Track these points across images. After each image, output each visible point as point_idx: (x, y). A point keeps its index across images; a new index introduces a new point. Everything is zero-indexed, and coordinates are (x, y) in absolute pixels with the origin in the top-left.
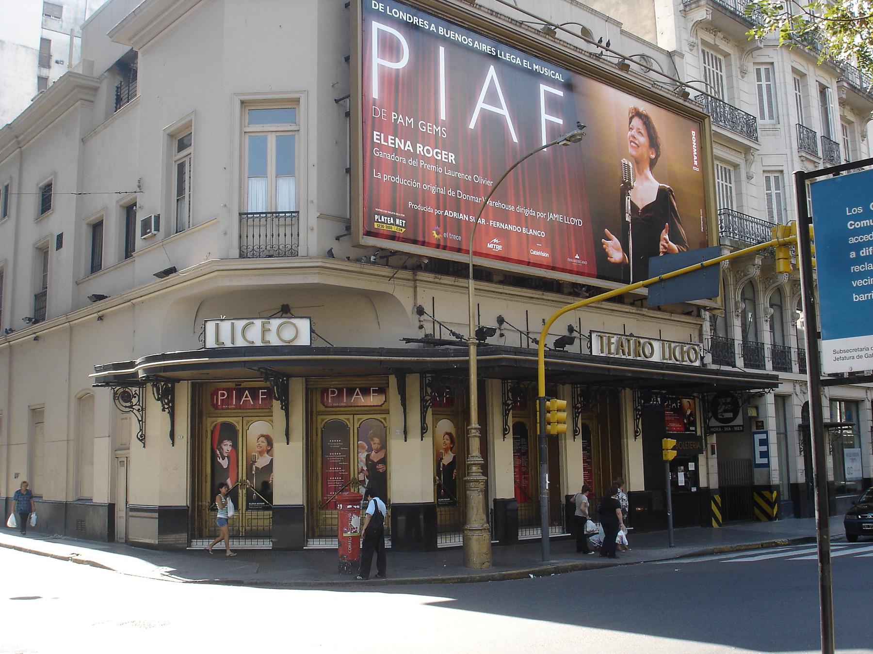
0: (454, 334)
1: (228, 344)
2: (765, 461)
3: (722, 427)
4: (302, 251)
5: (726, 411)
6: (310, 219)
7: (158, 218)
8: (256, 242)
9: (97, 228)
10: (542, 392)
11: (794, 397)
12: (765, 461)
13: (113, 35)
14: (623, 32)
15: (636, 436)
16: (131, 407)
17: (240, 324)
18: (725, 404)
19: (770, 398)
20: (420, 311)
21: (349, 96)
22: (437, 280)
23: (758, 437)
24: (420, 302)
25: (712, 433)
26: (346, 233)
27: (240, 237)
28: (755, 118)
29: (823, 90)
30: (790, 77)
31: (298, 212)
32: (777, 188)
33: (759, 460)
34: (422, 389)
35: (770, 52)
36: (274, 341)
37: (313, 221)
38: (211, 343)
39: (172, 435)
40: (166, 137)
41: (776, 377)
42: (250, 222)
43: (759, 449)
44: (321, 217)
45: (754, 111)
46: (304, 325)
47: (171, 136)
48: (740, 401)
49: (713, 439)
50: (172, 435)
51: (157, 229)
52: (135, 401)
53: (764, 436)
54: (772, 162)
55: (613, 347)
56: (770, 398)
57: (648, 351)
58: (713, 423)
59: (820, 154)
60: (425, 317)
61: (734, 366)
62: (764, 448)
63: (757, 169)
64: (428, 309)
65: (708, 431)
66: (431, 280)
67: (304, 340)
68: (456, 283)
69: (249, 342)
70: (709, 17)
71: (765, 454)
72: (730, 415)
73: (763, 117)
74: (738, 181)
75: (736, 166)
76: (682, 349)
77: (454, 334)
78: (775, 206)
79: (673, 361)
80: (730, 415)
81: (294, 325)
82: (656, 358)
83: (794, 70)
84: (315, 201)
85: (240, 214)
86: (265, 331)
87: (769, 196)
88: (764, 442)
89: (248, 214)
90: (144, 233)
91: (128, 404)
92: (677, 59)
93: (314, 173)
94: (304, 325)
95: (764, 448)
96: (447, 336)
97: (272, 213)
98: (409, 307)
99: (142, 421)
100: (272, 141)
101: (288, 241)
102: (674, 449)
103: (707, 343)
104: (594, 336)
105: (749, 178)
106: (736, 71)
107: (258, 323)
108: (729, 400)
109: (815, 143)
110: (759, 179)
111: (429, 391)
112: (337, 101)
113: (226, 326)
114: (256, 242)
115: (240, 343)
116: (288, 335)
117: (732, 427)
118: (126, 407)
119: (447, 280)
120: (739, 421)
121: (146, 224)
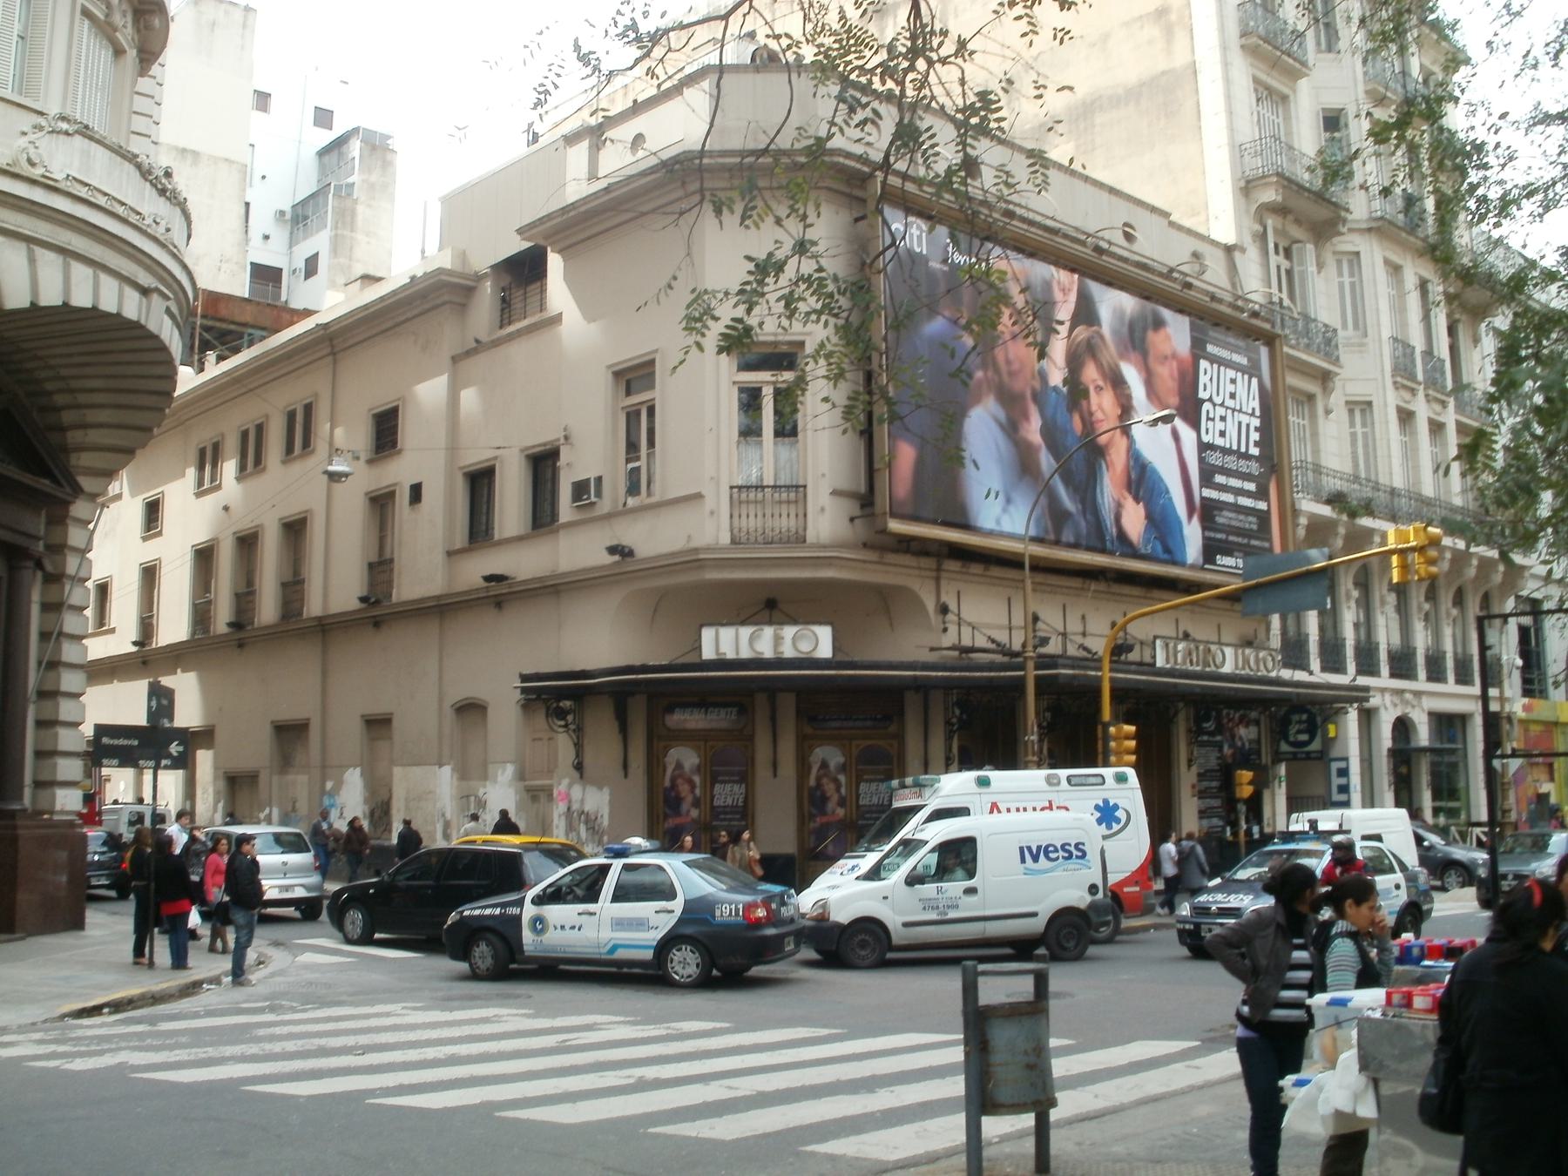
0: (993, 641)
1: (730, 655)
2: (1343, 797)
3: (1295, 754)
4: (811, 537)
5: (1299, 732)
7: (599, 480)
9: (480, 482)
10: (1107, 714)
11: (1382, 711)
12: (1343, 797)
13: (520, 231)
14: (1172, 224)
15: (1189, 766)
16: (566, 726)
17: (746, 632)
18: (1300, 722)
19: (1352, 717)
20: (944, 610)
23: (1335, 766)
24: (944, 598)
25: (1280, 761)
28: (1335, 331)
29: (1423, 285)
30: (1381, 273)
32: (1364, 425)
33: (1336, 797)
34: (946, 709)
35: (1356, 238)
36: (788, 652)
38: (708, 653)
39: (625, 766)
40: (610, 376)
41: (1366, 689)
43: (1336, 781)
44: (835, 493)
45: (1335, 322)
46: (824, 634)
47: (617, 375)
48: (1319, 719)
49: (1282, 769)
50: (625, 766)
51: (599, 494)
52: (570, 718)
53: (1342, 765)
54: (1358, 390)
55: (1180, 656)
56: (1352, 717)
57: (1219, 659)
58: (1284, 747)
59: (1420, 377)
61: (1311, 673)
62: (1343, 781)
63: (1337, 399)
64: (953, 606)
65: (1277, 758)
67: (825, 651)
70: (1279, 199)
71: (1344, 789)
72: (1304, 737)
73: (1345, 326)
74: (1313, 417)
75: (1311, 398)
76: (1257, 657)
78: (1360, 451)
79: (1248, 671)
80: (1304, 737)
82: (1227, 669)
83: (1387, 262)
86: (778, 640)
87: (1353, 435)
88: (1344, 772)
92: (1237, 254)
94: (824, 634)
95: (1343, 781)
96: (981, 642)
98: (931, 605)
99: (579, 747)
100: (768, 392)
102: (1250, 783)
103: (1276, 641)
104: (1158, 642)
105: (1328, 412)
106: (1312, 268)
107: (768, 631)
108: (1304, 717)
109: (1413, 361)
110: (1340, 413)
111: (957, 712)
113: (727, 633)
115: (745, 654)
116: (805, 647)
117: (1308, 753)
119: (976, 569)
120: (1316, 746)
121: (580, 489)
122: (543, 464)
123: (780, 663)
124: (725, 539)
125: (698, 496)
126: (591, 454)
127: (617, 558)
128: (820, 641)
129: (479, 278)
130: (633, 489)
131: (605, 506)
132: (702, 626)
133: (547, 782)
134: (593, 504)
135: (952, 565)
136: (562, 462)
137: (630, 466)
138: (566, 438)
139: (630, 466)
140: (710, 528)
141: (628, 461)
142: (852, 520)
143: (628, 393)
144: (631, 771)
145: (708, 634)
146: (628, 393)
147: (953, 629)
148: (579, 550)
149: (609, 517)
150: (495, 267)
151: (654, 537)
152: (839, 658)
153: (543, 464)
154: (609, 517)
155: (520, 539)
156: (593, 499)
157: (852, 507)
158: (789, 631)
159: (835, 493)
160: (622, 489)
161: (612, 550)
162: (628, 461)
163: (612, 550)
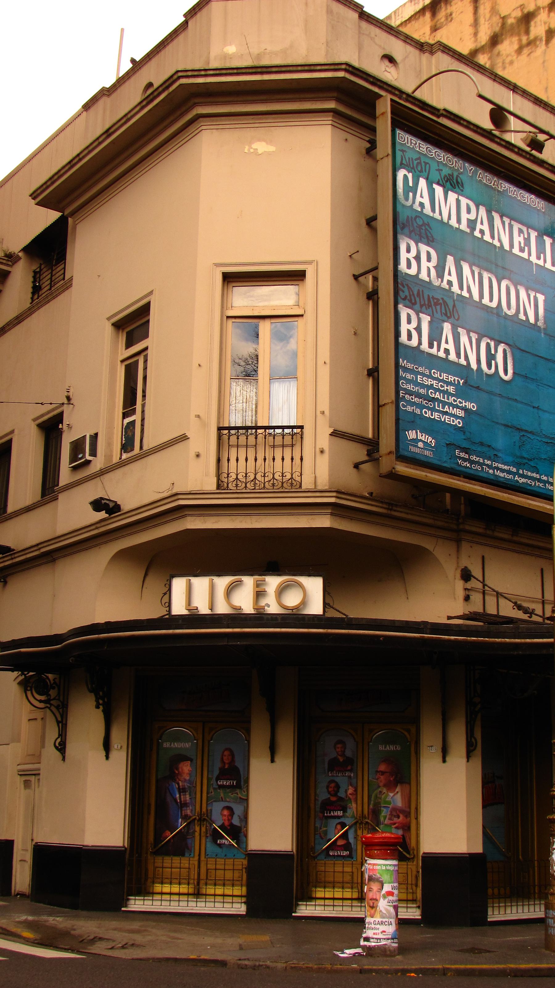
1: (204, 610)
4: (307, 483)
6: (318, 437)
7: (95, 437)
8: (242, 469)
17: (222, 582)
21: (376, 268)
22: (489, 532)
26: (366, 458)
27: (219, 461)
31: (301, 427)
36: (273, 607)
37: (324, 440)
38: (179, 608)
39: (107, 746)
42: (233, 439)
44: (335, 434)
46: (314, 586)
47: (118, 326)
51: (94, 453)
52: (53, 693)
60: (473, 584)
64: (476, 572)
66: (481, 531)
67: (316, 607)
68: (515, 538)
69: (235, 608)
77: (520, 607)
81: (301, 585)
84: (327, 412)
85: (220, 429)
86: (259, 594)
89: (230, 428)
90: (74, 457)
91: (43, 698)
93: (325, 373)
94: (314, 586)
96: (507, 610)
97: (265, 428)
101: (287, 469)
107: (249, 581)
112: (356, 278)
113: (201, 584)
114: (242, 469)
115: (222, 608)
116: (292, 599)
118: (40, 701)
121: (77, 447)
122: (51, 428)
123: (260, 618)
124: (211, 485)
125: (184, 438)
126: (95, 415)
127: (103, 515)
128: (310, 594)
129: (11, 258)
130: (127, 446)
131: (98, 464)
132: (173, 576)
133: (36, 766)
134: (88, 462)
135: (477, 527)
136: (64, 426)
137: (127, 421)
138: (68, 398)
139: (127, 421)
140: (192, 472)
141: (125, 416)
142: (356, 466)
143: (129, 344)
144: (114, 754)
145: (179, 585)
146: (129, 344)
147: (477, 598)
148: (74, 512)
149: (102, 473)
150: (25, 250)
151: (137, 488)
152: (332, 614)
153: (51, 428)
154: (102, 473)
155: (28, 509)
156: (88, 457)
157: (359, 453)
158: (273, 582)
159: (335, 434)
160: (117, 446)
161: (98, 505)
162: (125, 416)
163: (98, 505)
